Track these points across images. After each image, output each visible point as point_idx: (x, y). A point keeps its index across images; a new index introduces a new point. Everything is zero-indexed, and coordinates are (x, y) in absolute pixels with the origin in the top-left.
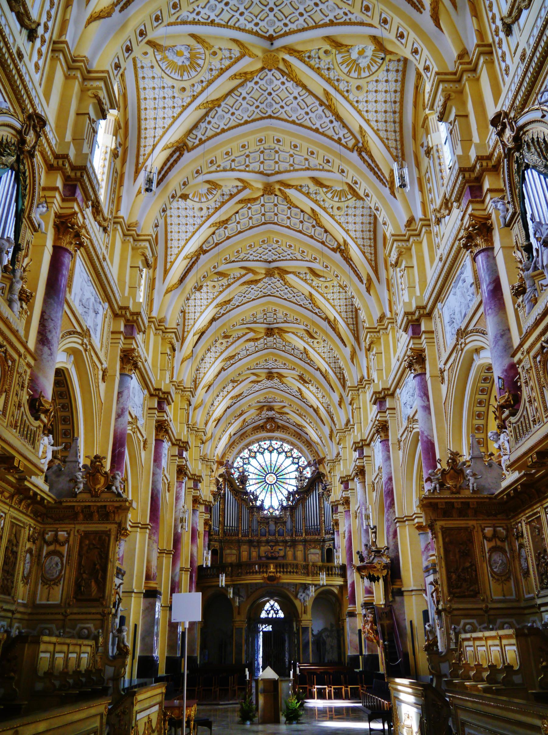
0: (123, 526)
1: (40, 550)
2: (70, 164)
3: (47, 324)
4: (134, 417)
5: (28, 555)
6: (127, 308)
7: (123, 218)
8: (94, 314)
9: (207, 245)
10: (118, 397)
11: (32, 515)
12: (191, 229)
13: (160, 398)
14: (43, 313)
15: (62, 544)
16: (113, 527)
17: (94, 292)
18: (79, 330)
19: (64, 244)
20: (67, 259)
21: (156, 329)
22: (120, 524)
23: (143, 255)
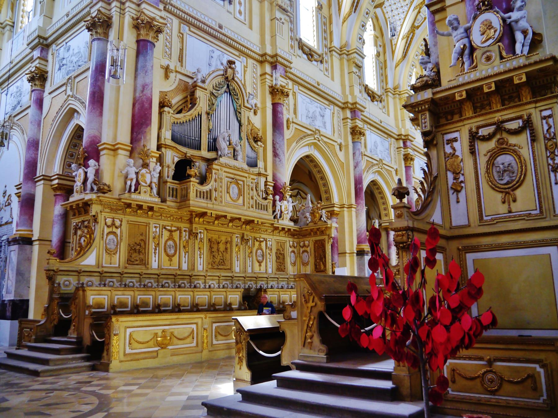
0: (330, 236)
1: (299, 250)
2: (270, 56)
3: (275, 146)
4: (378, 160)
5: (292, 254)
6: (347, 103)
7: (334, 47)
8: (322, 117)
9: (418, 22)
10: (354, 156)
11: (290, 236)
12: (402, 16)
13: (403, 140)
14: (273, 140)
15: (308, 247)
16: (326, 237)
17: (319, 105)
18: (309, 132)
19: (276, 101)
20: (279, 109)
21: (394, 95)
22: (329, 235)
23: (354, 63)
